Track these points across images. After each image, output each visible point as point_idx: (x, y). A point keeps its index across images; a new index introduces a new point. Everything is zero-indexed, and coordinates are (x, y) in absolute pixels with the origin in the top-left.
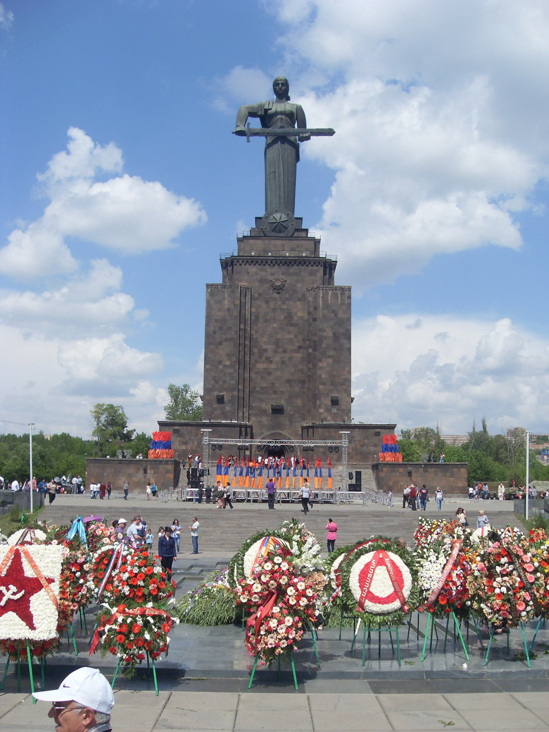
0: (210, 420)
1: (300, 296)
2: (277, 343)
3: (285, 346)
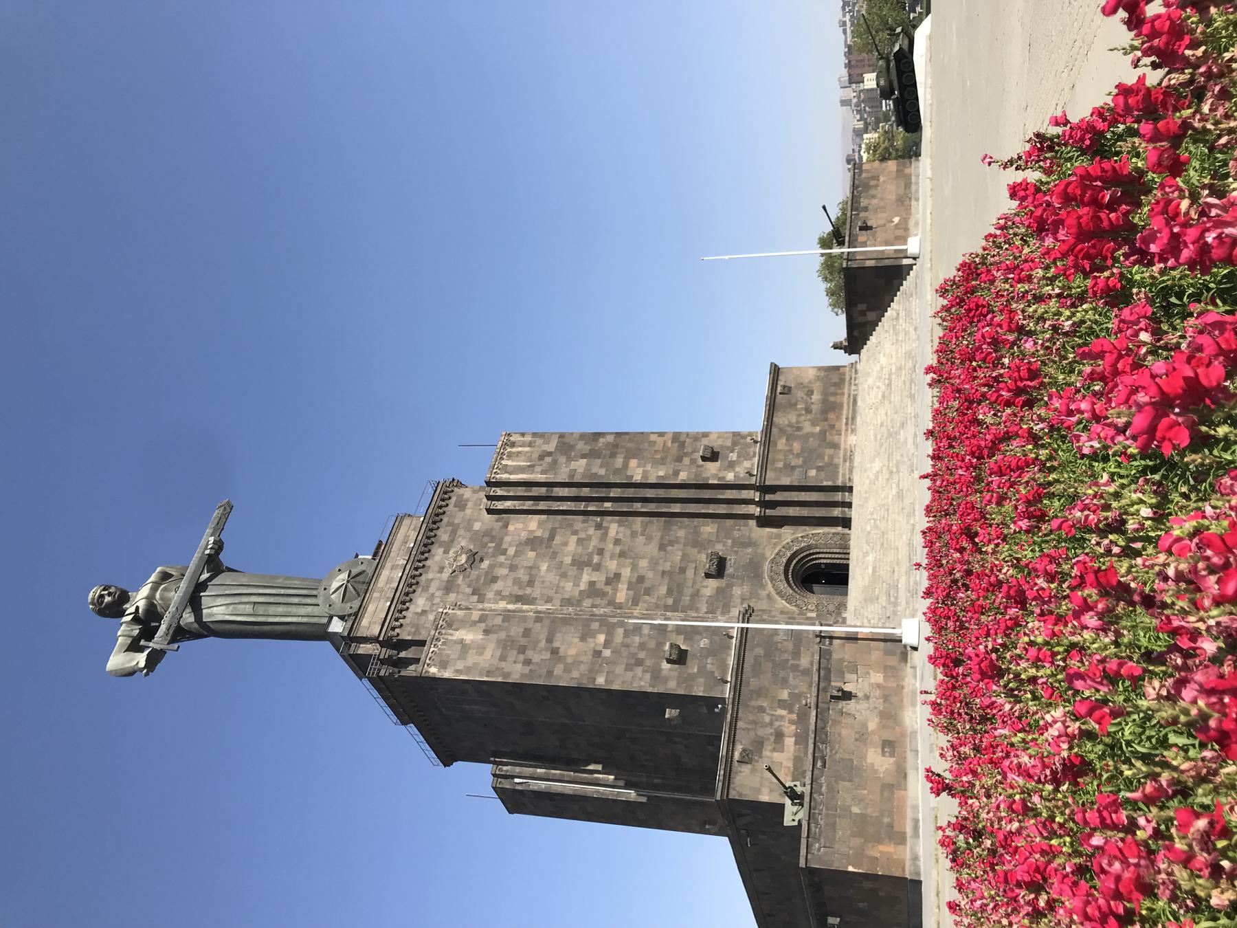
0: (726, 682)
2: (580, 564)
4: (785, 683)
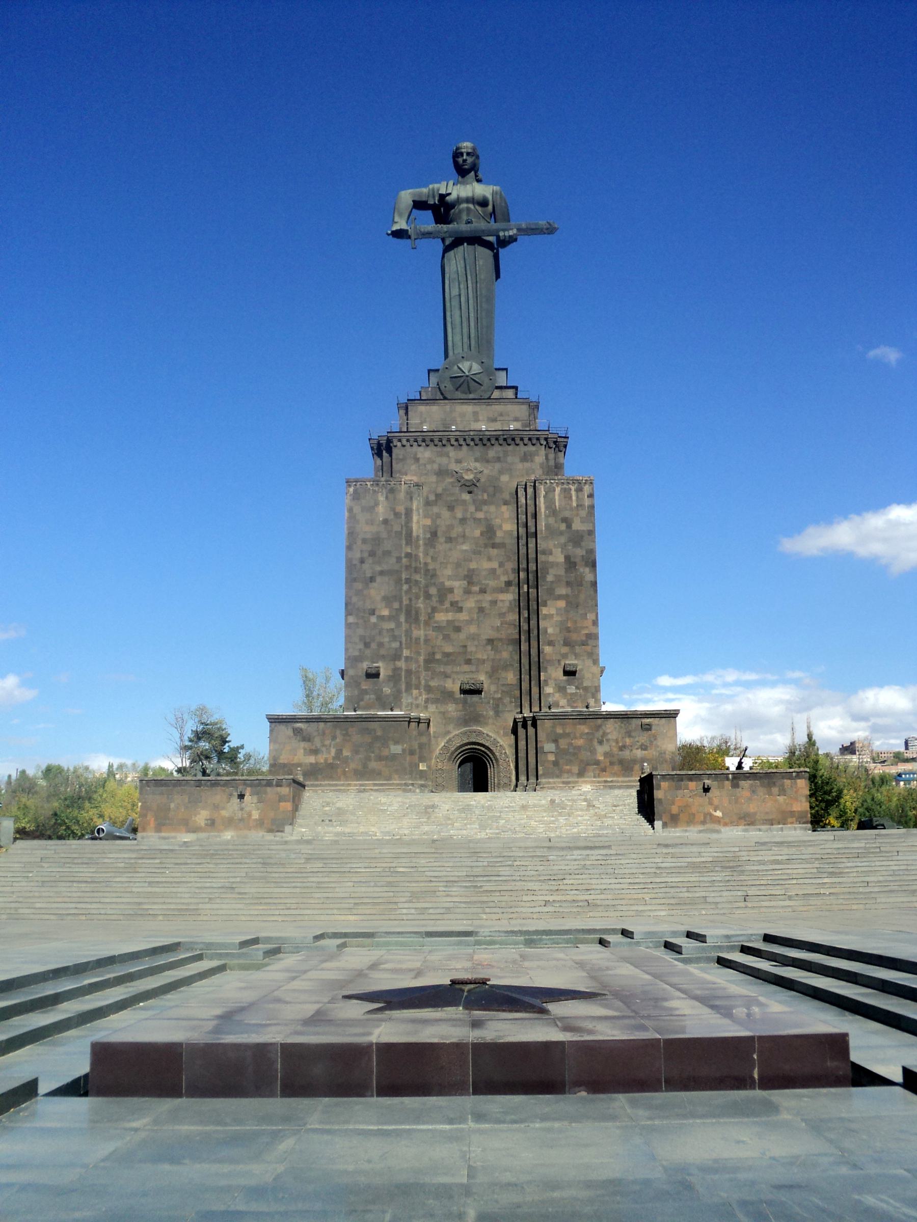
1: (506, 496)
2: (470, 577)
3: (483, 582)
4: (356, 752)
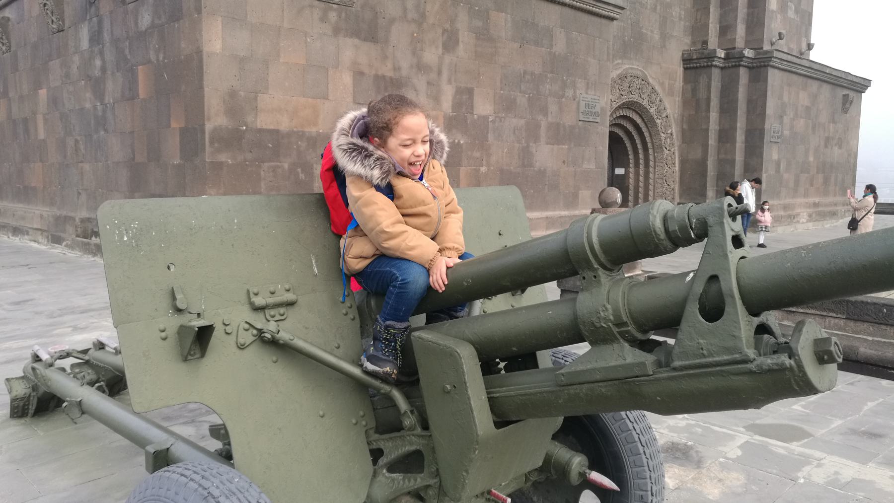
4: (507, 106)
